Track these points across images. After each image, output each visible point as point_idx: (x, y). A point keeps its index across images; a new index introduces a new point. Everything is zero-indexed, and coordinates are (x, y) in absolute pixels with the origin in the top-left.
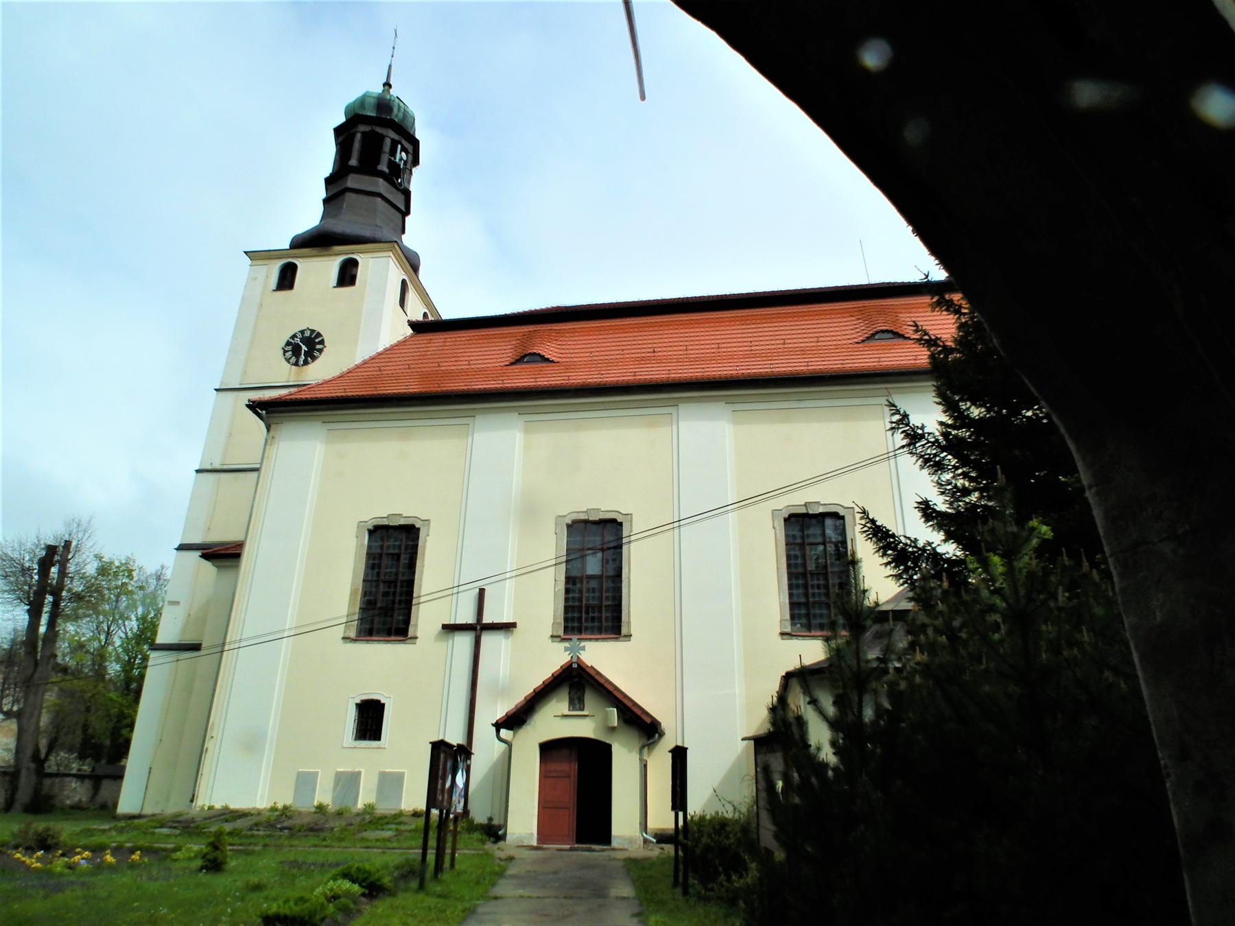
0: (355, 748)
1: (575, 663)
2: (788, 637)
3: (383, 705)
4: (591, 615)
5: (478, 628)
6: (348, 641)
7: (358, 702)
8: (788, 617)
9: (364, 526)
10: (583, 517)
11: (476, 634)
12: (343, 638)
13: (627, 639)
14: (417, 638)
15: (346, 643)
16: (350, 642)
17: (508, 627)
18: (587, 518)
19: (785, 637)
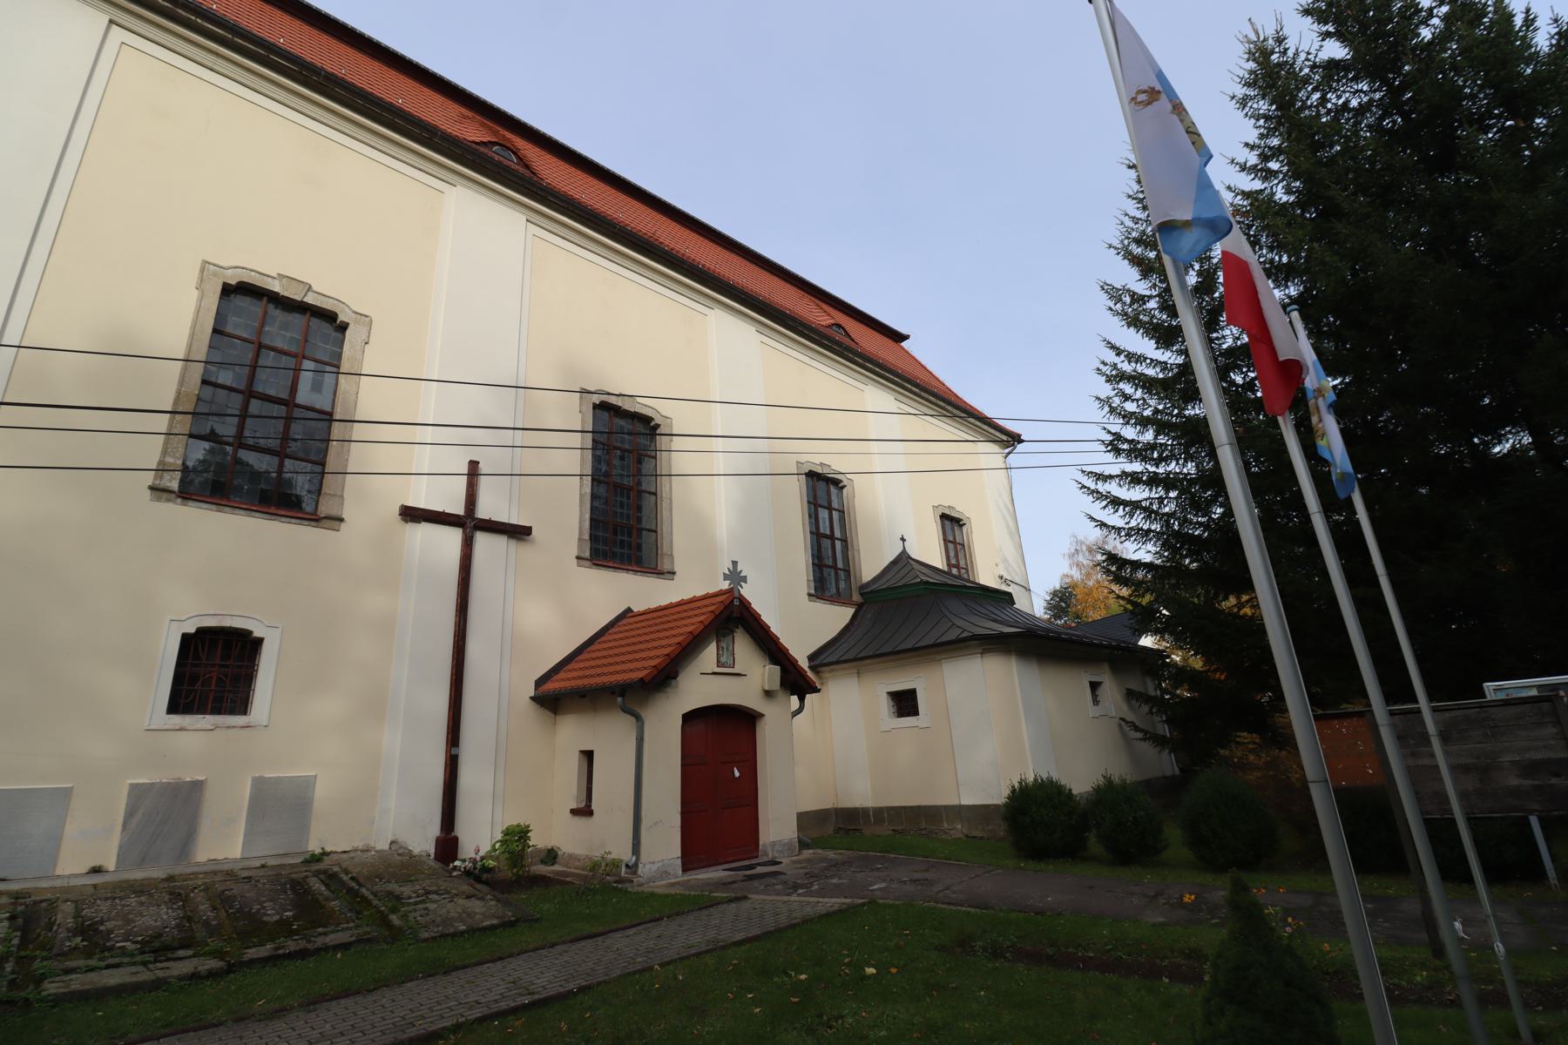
0: (181, 729)
1: (736, 598)
2: (815, 599)
3: (260, 641)
4: (619, 537)
5: (469, 523)
6: (165, 495)
7: (192, 630)
8: (812, 578)
9: (215, 274)
10: (613, 400)
11: (464, 532)
12: (152, 488)
13: (670, 576)
14: (342, 520)
15: (159, 499)
16: (168, 500)
17: (519, 533)
18: (620, 404)
19: (812, 598)
